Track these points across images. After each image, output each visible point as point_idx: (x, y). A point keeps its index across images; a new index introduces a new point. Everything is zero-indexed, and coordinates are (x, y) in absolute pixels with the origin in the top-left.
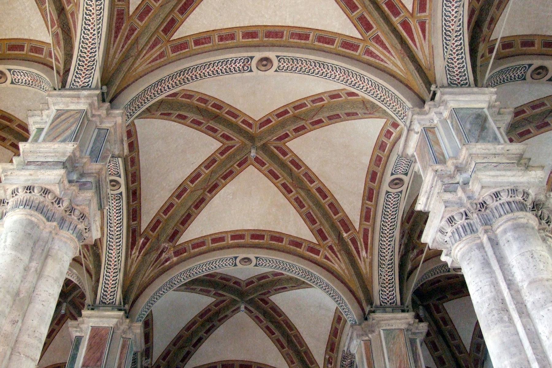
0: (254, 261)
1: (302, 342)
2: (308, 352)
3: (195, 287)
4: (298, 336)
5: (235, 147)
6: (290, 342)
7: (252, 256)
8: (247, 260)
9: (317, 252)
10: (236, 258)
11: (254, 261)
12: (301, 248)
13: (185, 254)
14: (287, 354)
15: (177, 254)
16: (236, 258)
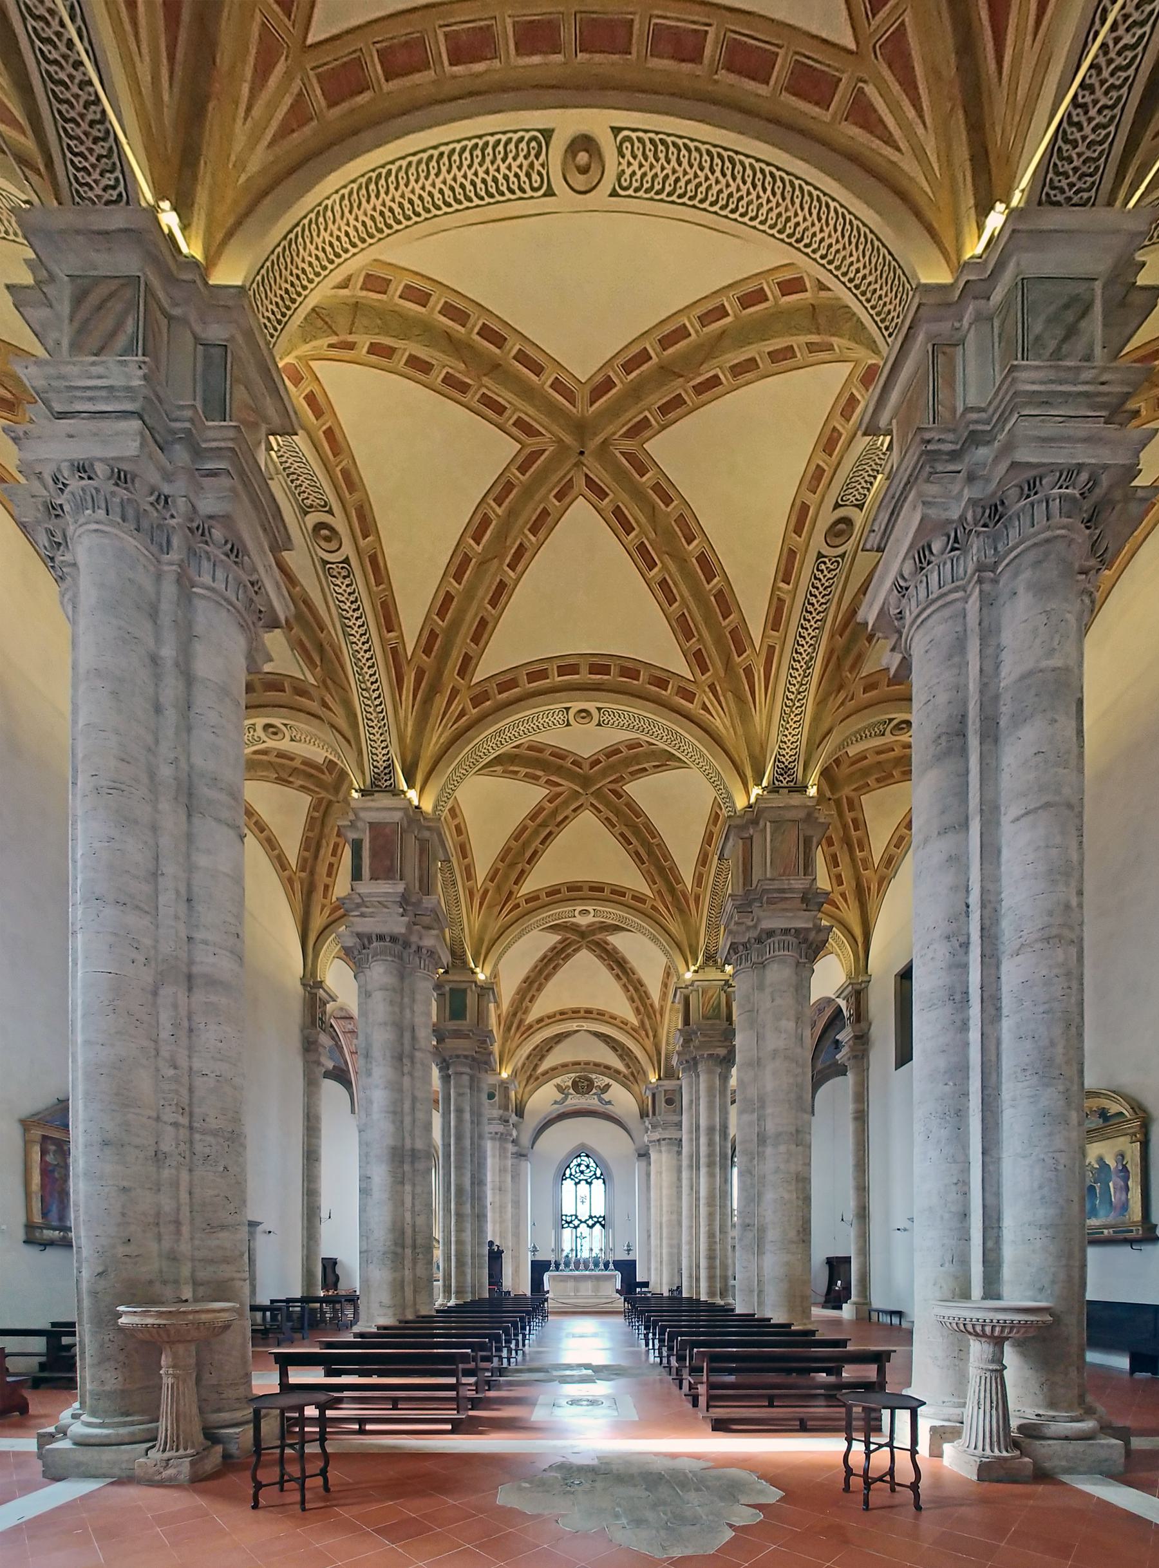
0: (595, 713)
1: (667, 856)
2: (673, 868)
3: (516, 769)
4: (662, 846)
5: (547, 453)
6: (650, 853)
7: (591, 706)
8: (585, 714)
9: (689, 696)
10: (567, 709)
11: (595, 713)
12: (666, 690)
13: (488, 703)
14: (649, 872)
15: (476, 701)
16: (567, 709)
